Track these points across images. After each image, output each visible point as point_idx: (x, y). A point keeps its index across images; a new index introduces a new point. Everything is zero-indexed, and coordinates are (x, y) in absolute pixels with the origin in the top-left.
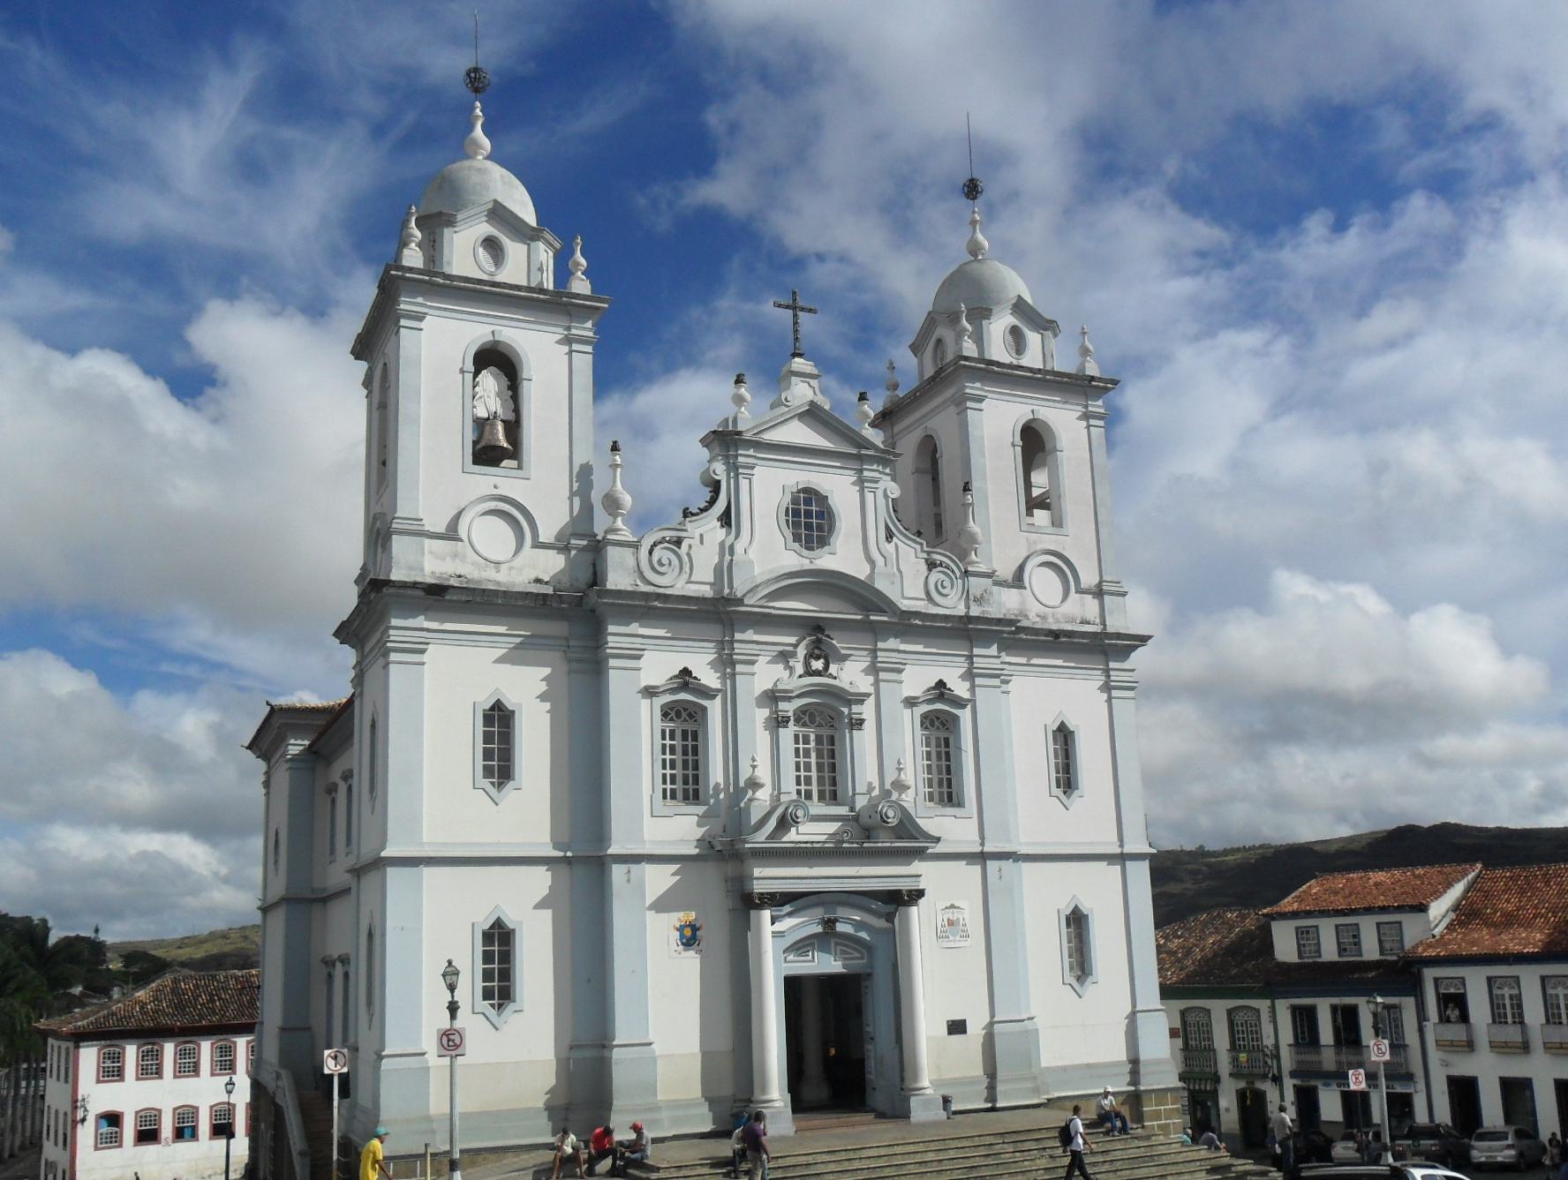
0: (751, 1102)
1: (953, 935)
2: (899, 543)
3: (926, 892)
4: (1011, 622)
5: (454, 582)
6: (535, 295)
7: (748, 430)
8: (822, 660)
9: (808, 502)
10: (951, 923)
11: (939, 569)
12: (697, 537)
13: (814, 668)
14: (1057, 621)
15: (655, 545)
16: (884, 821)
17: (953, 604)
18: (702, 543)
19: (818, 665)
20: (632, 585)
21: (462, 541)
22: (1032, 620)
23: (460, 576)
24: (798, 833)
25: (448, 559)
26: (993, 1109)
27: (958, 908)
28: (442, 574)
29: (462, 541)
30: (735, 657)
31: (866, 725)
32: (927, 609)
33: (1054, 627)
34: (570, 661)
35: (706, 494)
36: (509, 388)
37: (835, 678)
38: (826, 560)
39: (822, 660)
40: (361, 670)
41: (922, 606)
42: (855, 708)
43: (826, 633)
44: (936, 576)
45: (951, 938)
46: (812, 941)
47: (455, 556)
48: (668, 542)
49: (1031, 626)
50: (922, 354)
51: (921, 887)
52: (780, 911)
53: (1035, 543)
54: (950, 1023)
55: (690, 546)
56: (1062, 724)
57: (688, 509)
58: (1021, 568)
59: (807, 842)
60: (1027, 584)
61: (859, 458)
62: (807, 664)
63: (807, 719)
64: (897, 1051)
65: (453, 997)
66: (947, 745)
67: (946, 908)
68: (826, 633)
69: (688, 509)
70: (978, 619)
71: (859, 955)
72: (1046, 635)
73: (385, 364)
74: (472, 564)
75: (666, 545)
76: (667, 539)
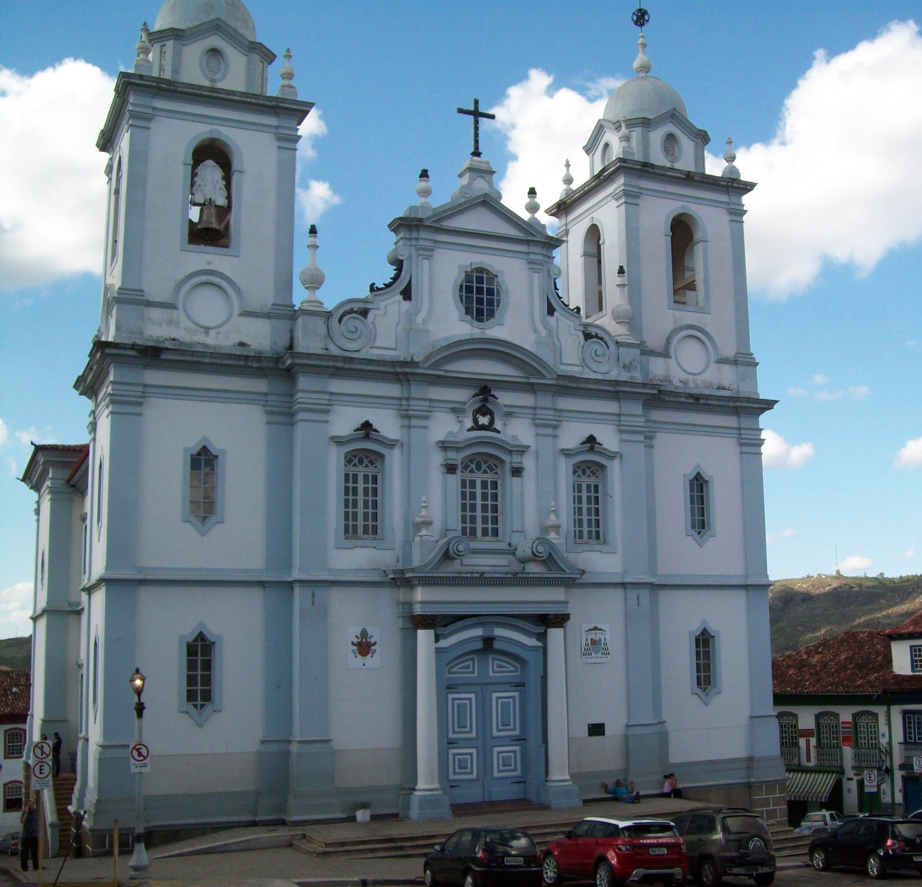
0: (415, 790)
1: (595, 653)
3: (571, 616)
4: (654, 386)
5: (168, 345)
7: (428, 218)
8: (488, 417)
10: (594, 642)
11: (594, 339)
13: (480, 423)
14: (697, 387)
15: (345, 314)
16: (534, 555)
18: (385, 314)
19: (484, 420)
23: (174, 340)
24: (462, 565)
25: (164, 325)
27: (601, 630)
28: (158, 337)
30: (410, 412)
31: (525, 473)
32: (582, 374)
33: (693, 392)
34: (268, 413)
35: (391, 271)
36: (223, 179)
37: (499, 432)
38: (495, 331)
39: (488, 417)
40: (95, 418)
41: (576, 371)
42: (516, 458)
43: (493, 393)
44: (594, 345)
45: (593, 655)
47: (170, 322)
48: (356, 312)
49: (674, 390)
50: (593, 155)
51: (568, 613)
54: (591, 726)
55: (375, 316)
58: (668, 342)
59: (467, 573)
60: (672, 354)
61: (527, 242)
62: (475, 421)
63: (473, 466)
64: (543, 750)
65: (139, 699)
66: (596, 491)
67: (590, 630)
68: (493, 393)
69: (373, 284)
70: (625, 383)
71: (511, 668)
72: (686, 398)
73: (120, 157)
74: (185, 329)
75: (354, 315)
76: (355, 309)
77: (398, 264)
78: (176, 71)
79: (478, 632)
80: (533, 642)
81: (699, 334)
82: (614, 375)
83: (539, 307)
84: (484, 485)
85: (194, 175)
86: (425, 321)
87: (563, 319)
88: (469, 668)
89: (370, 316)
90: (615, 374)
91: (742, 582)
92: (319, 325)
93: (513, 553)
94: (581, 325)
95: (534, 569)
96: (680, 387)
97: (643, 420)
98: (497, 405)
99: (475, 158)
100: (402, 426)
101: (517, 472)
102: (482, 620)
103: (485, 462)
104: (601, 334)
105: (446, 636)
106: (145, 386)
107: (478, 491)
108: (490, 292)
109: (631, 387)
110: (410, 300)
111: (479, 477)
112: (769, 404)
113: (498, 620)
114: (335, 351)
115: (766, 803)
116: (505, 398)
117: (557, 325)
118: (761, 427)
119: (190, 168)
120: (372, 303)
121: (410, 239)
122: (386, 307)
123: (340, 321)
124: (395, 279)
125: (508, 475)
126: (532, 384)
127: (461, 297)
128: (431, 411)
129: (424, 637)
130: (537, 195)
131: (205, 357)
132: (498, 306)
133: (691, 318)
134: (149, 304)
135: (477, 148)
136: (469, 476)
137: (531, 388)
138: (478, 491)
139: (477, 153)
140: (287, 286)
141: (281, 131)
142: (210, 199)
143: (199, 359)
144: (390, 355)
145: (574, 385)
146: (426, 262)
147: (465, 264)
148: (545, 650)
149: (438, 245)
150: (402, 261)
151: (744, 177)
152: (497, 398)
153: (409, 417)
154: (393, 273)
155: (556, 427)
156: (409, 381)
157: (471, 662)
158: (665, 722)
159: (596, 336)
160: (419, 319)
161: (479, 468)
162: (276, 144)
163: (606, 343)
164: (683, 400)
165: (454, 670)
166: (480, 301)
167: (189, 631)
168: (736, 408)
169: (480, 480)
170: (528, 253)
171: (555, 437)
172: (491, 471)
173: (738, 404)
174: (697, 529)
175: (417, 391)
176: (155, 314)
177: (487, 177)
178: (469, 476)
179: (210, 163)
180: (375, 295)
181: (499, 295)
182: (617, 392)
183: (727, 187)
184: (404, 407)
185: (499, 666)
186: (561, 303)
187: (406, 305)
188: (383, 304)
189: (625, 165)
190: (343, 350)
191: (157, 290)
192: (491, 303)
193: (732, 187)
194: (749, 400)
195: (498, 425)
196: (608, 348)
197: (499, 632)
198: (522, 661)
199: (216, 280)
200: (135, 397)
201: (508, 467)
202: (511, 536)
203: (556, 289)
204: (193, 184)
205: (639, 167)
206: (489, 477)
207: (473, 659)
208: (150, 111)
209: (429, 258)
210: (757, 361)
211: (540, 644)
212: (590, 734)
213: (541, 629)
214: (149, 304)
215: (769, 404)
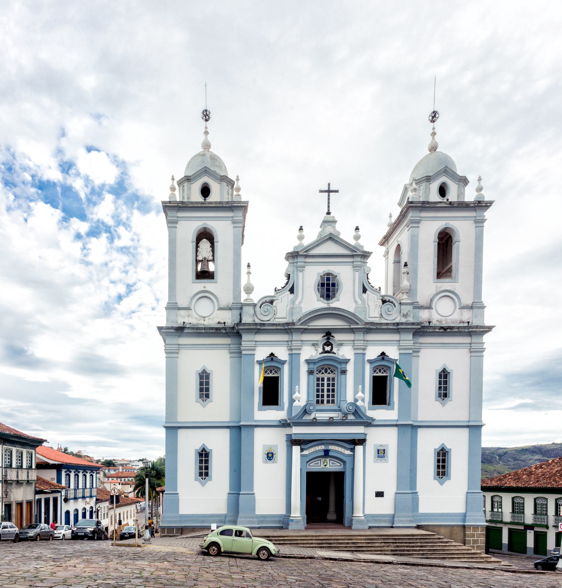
2: (369, 293)
6: (218, 205)
8: (330, 346)
9: (328, 279)
11: (388, 303)
12: (280, 299)
13: (326, 350)
15: (262, 304)
17: (395, 317)
19: (328, 348)
20: (252, 321)
21: (191, 310)
22: (435, 323)
23: (190, 324)
25: (186, 317)
26: (392, 527)
29: (191, 310)
30: (292, 347)
37: (335, 354)
38: (334, 304)
39: (330, 346)
41: (377, 320)
42: (343, 366)
46: (320, 459)
48: (268, 302)
52: (306, 447)
53: (440, 287)
54: (377, 493)
55: (277, 303)
56: (444, 369)
57: (276, 288)
61: (353, 256)
62: (324, 349)
69: (276, 288)
71: (339, 464)
72: (439, 329)
74: (195, 318)
75: (267, 304)
76: (267, 301)
77: (288, 277)
78: (189, 198)
79: (323, 447)
80: (348, 452)
81: (450, 295)
82: (397, 321)
83: (358, 289)
84: (329, 379)
85: (197, 247)
86: (300, 303)
87: (372, 295)
88: (318, 464)
89: (274, 303)
90: (399, 319)
91: (466, 424)
92: (250, 310)
93: (340, 411)
94: (381, 296)
95: (351, 417)
96: (437, 324)
97: (412, 342)
98: (334, 341)
99: (329, 216)
100: (289, 354)
101: (344, 372)
102: (323, 442)
103: (329, 369)
104: (392, 300)
105: (306, 449)
106: (179, 345)
107: (326, 382)
108: (334, 285)
109: (406, 325)
110: (293, 293)
111: (326, 376)
112: (490, 328)
113: (332, 442)
114: (257, 321)
115: (473, 536)
116: (338, 337)
117: (368, 296)
118: (484, 342)
119: (195, 244)
120: (275, 297)
121: (293, 263)
122: (281, 298)
123: (260, 307)
124: (287, 284)
125: (339, 374)
126: (352, 329)
127: (318, 289)
128: (302, 346)
129: (296, 449)
130: (360, 230)
131: (202, 330)
132: (337, 292)
133: (445, 284)
134: (179, 309)
135: (329, 210)
136: (320, 376)
137: (352, 331)
138: (326, 382)
139: (328, 213)
140: (237, 295)
141: (234, 218)
142: (205, 258)
143: (200, 331)
144: (285, 321)
145: (375, 327)
146: (301, 274)
147: (321, 272)
148: (354, 455)
149: (306, 264)
150: (289, 275)
151: (487, 199)
152: (334, 337)
153: (292, 350)
154: (286, 281)
155: (364, 349)
156: (292, 332)
157: (319, 461)
158: (417, 493)
159: (389, 301)
160: (297, 302)
161: (326, 371)
162: (232, 226)
163: (394, 304)
164: (437, 330)
165: (310, 465)
166: (328, 290)
167: (198, 447)
168: (470, 332)
169: (327, 377)
170: (353, 262)
171: (364, 354)
172: (332, 373)
173: (470, 330)
174: (442, 398)
175: (296, 337)
176: (182, 312)
177: (333, 224)
178: (320, 376)
179: (205, 240)
180: (276, 293)
181: (338, 286)
182: (398, 329)
183: (474, 207)
184: (289, 345)
185: (332, 463)
186: (370, 287)
187: (292, 296)
188: (280, 297)
189: (412, 205)
190: (262, 321)
191: (182, 302)
192: (334, 291)
193: (478, 206)
194: (477, 327)
195: (335, 350)
196: (395, 307)
197: (331, 447)
198: (344, 462)
199: (208, 295)
200: (176, 350)
201: (339, 370)
202: (340, 402)
203: (368, 279)
204: (197, 251)
205: (420, 205)
206: (331, 376)
207: (320, 460)
208: (176, 219)
209: (302, 271)
210: (485, 305)
211: (352, 453)
212: (376, 496)
213: (352, 446)
214: (179, 309)
215: (489, 329)
